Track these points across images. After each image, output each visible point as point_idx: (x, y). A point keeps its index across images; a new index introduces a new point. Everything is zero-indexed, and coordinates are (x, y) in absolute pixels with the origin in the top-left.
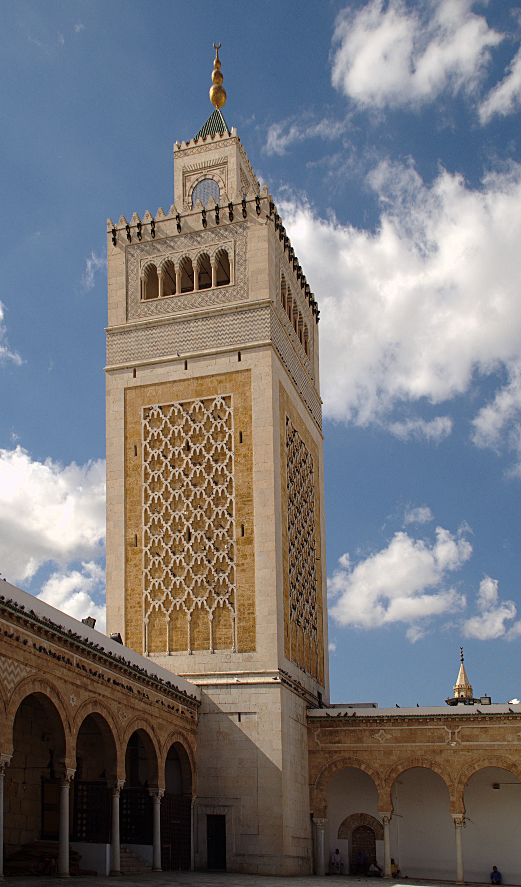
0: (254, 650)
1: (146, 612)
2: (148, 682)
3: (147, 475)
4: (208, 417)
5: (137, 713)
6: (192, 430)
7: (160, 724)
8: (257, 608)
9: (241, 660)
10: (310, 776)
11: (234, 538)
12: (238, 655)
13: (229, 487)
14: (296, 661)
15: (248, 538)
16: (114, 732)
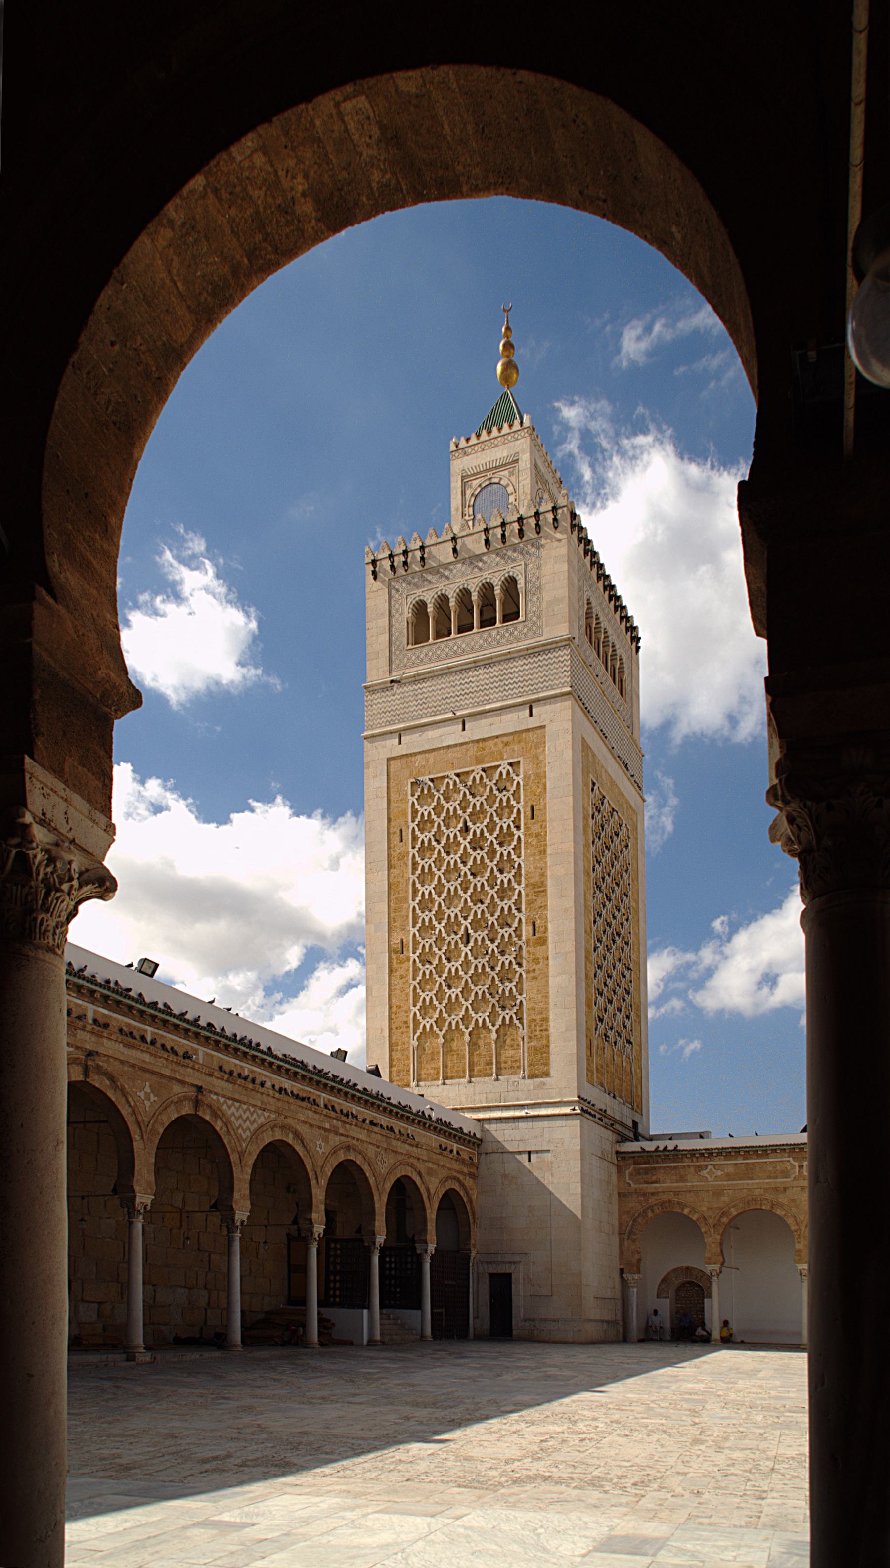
0: (547, 1074)
1: (415, 1033)
2: (414, 1120)
3: (415, 865)
4: (491, 789)
5: (400, 1157)
6: (471, 807)
7: (430, 1169)
8: (551, 1023)
9: (531, 1087)
10: (620, 1224)
11: (524, 938)
12: (528, 1082)
13: (518, 875)
14: (602, 1085)
15: (540, 938)
16: (372, 1180)
